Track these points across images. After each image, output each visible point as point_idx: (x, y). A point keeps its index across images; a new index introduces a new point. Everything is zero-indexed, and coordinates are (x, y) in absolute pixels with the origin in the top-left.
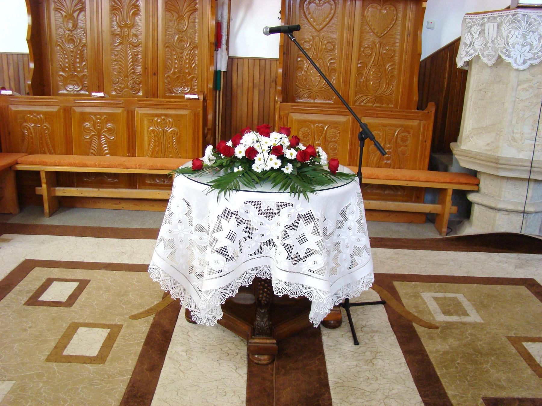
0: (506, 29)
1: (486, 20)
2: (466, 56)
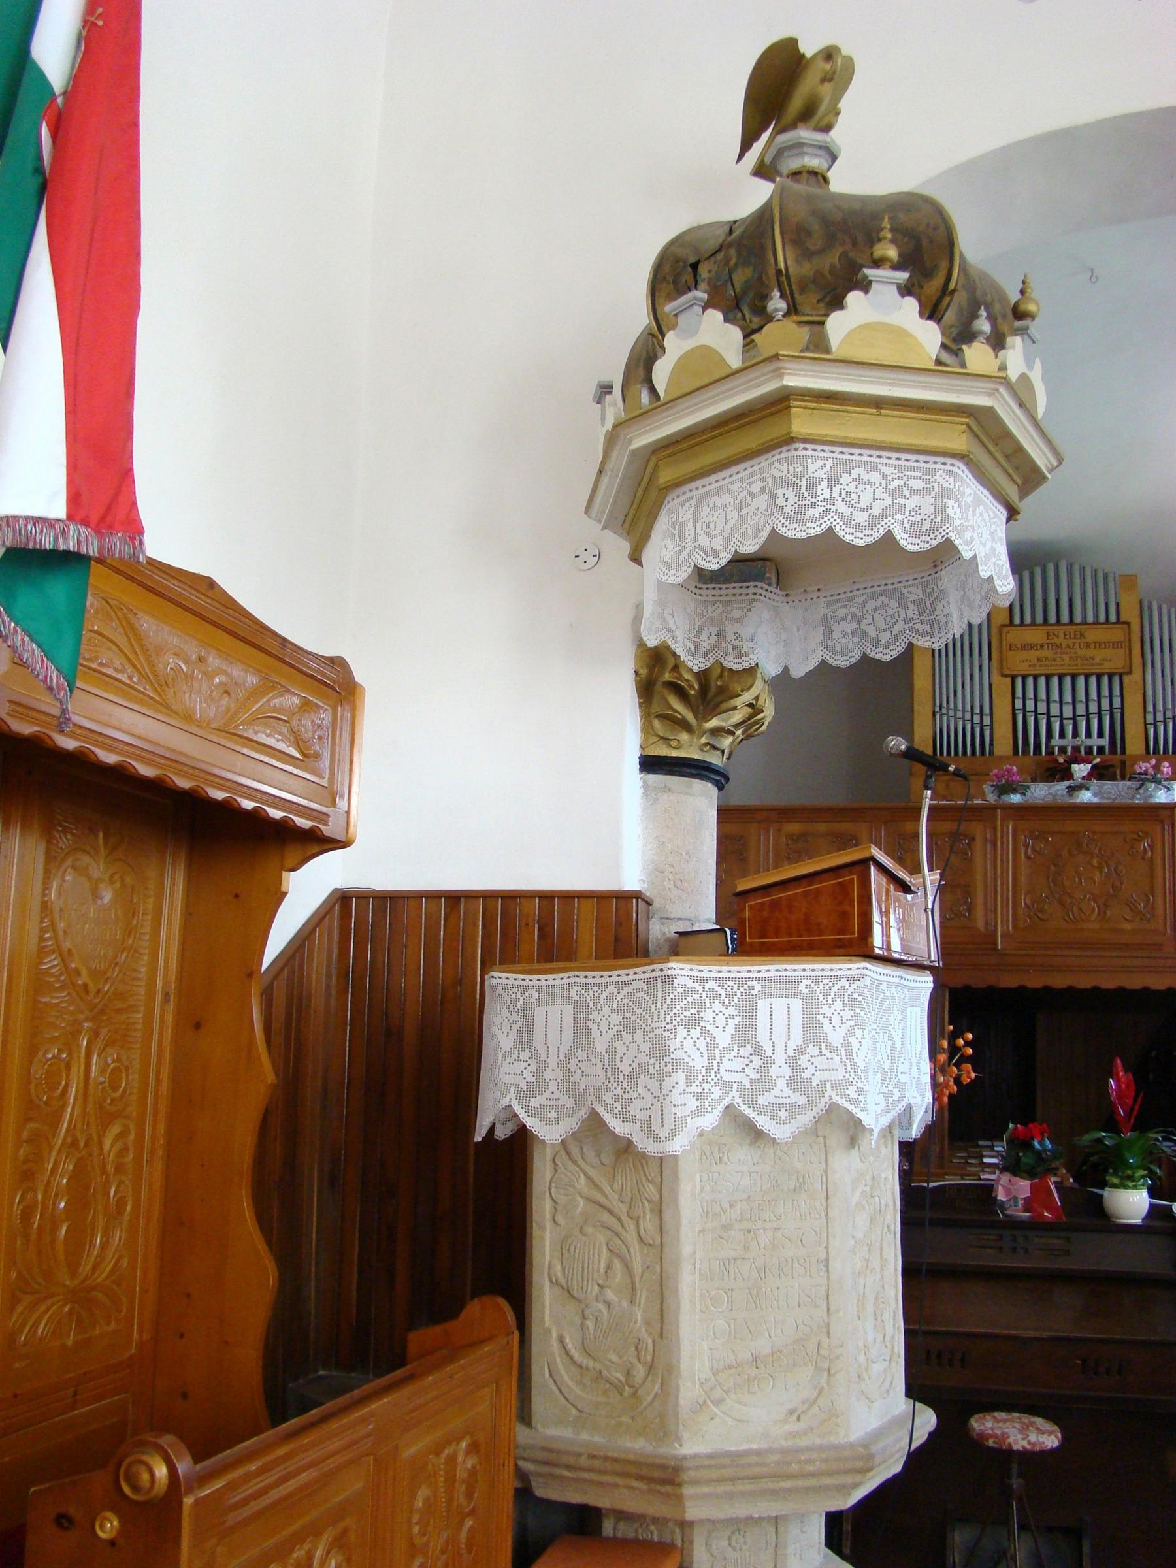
0: (836, 1020)
1: (758, 987)
2: (701, 1111)
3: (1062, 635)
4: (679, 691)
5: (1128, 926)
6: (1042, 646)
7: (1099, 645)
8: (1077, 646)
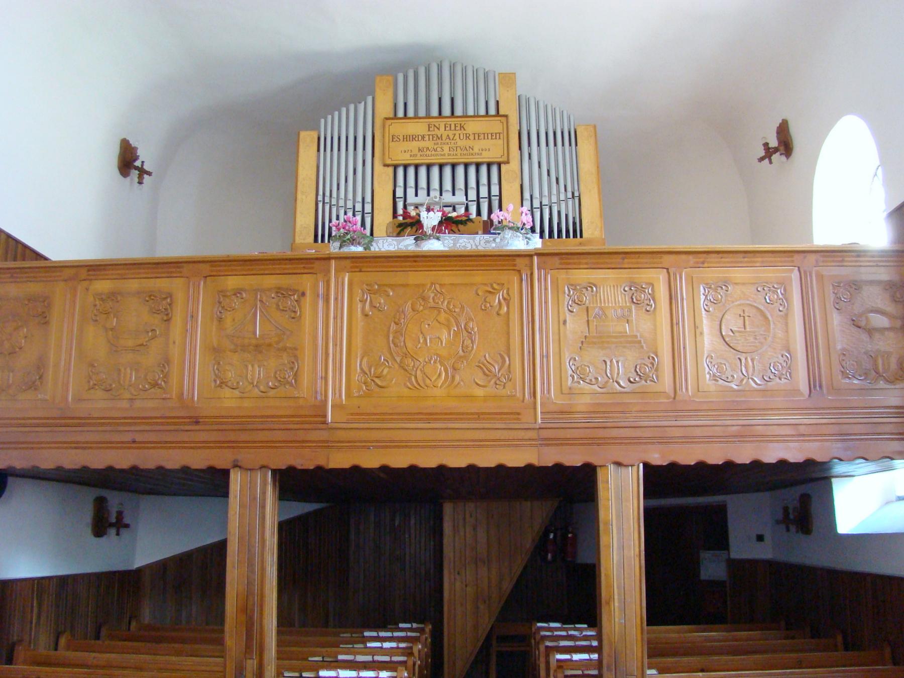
3: (442, 128)
5: (480, 392)
6: (423, 137)
7: (478, 136)
8: (457, 136)
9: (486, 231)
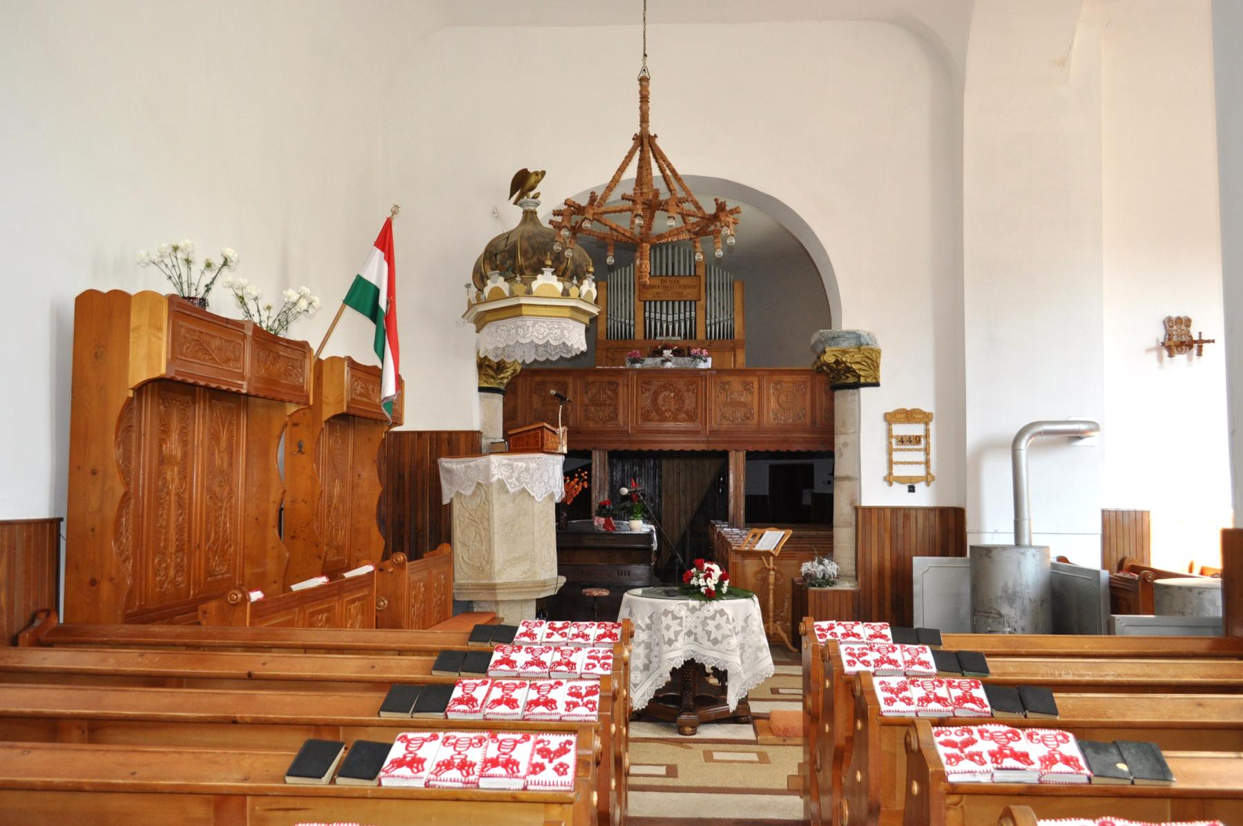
4: (490, 367)
7: (685, 287)
9: (689, 355)
